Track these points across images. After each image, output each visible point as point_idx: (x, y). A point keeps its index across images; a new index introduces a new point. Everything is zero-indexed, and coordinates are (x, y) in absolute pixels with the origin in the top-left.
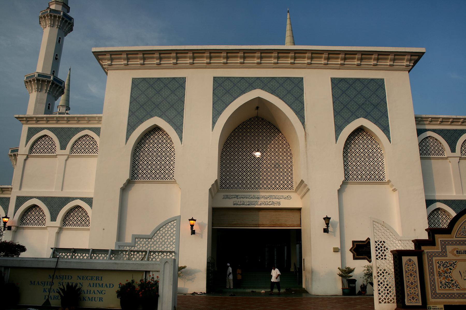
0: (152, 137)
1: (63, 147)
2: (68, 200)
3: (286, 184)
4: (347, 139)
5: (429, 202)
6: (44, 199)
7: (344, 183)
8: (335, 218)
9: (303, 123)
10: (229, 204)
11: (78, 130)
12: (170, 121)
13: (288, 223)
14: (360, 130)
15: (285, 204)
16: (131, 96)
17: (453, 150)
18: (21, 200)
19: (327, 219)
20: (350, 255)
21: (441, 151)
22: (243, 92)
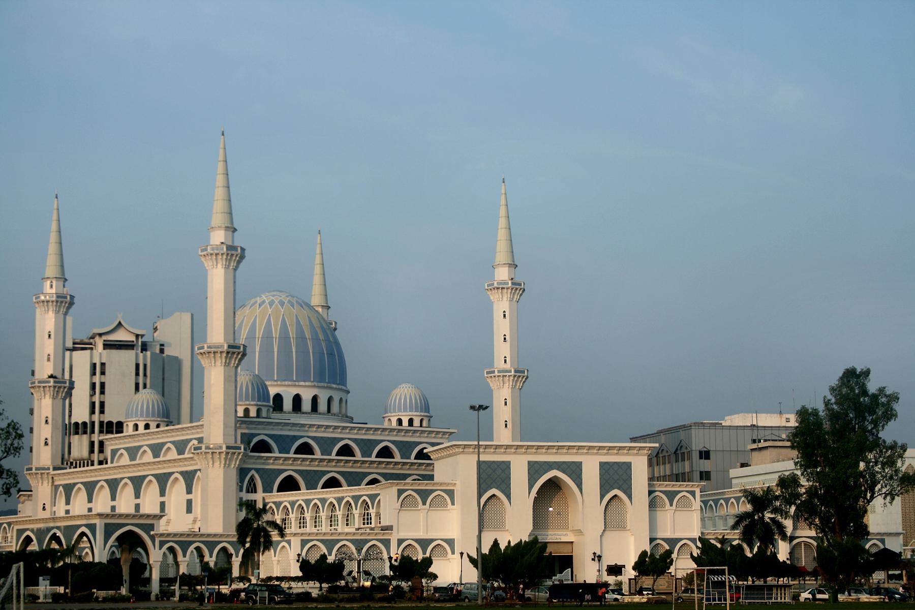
1: (424, 504)
2: (432, 540)
3: (566, 527)
5: (652, 540)
11: (433, 491)
13: (564, 551)
15: (564, 539)
17: (671, 505)
18: (400, 541)
19: (594, 553)
21: (663, 506)
22: (546, 472)
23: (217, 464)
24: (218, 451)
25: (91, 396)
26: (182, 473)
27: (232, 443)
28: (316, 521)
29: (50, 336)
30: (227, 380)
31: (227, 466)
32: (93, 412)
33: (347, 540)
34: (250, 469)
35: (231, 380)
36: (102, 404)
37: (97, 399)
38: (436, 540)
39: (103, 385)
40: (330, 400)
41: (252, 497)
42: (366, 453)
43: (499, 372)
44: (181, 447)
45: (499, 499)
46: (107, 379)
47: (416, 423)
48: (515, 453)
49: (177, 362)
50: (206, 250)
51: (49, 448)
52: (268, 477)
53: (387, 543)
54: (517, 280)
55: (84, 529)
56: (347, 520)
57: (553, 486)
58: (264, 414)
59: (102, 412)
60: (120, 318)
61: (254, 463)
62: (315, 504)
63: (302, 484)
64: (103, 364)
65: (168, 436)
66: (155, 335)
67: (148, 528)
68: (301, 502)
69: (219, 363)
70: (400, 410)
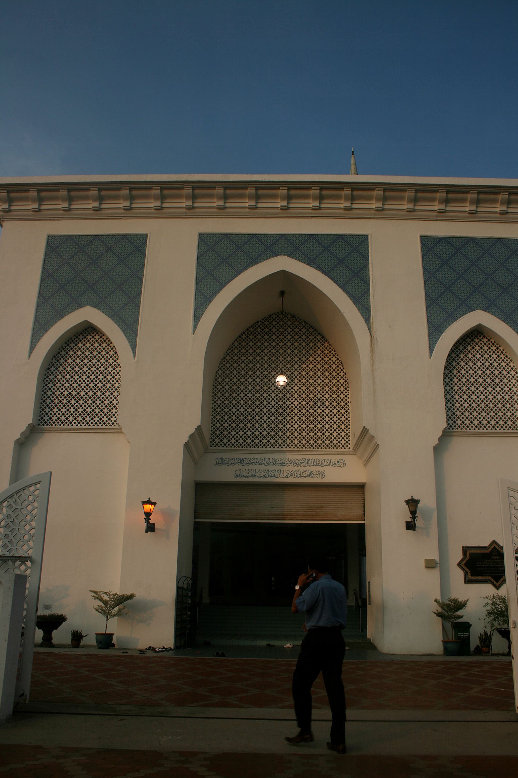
0: (80, 345)
4: (452, 351)
7: (447, 434)
8: (428, 502)
9: (367, 319)
10: (227, 474)
12: (115, 315)
13: (337, 512)
14: (476, 334)
15: (334, 475)
16: (43, 268)
20: (458, 575)
22: (254, 261)
48: (159, 213)
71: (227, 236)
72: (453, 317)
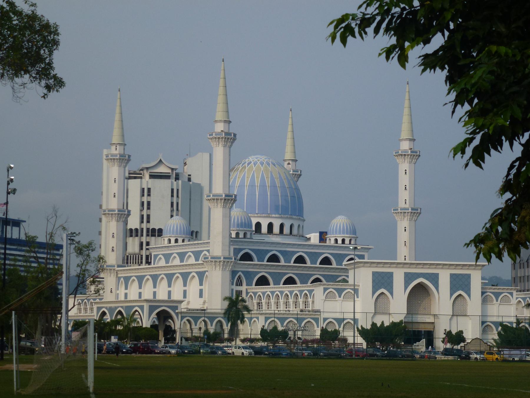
1: (340, 297)
6: (335, 319)
11: (345, 289)
13: (429, 328)
15: (428, 320)
17: (497, 301)
18: (325, 319)
21: (492, 301)
22: (416, 279)
23: (218, 268)
24: (218, 260)
25: (141, 210)
26: (197, 273)
27: (227, 255)
28: (277, 304)
29: (115, 181)
30: (224, 216)
31: (223, 270)
32: (142, 222)
33: (293, 318)
34: (238, 272)
35: (228, 217)
36: (148, 216)
37: (145, 213)
38: (347, 319)
39: (149, 203)
40: (291, 227)
41: (239, 288)
42: (313, 262)
43: (401, 209)
44: (197, 255)
45: (386, 295)
46: (152, 199)
47: (347, 241)
49: (199, 187)
50: (212, 135)
51: (114, 253)
52: (249, 275)
53: (317, 320)
54: (416, 149)
55: (137, 308)
56: (296, 305)
57: (421, 287)
58: (248, 236)
59: (148, 222)
60: (161, 157)
61: (241, 268)
62: (277, 294)
63: (271, 281)
64: (149, 190)
65: (190, 248)
66: (185, 167)
67: (175, 308)
68: (269, 293)
69: (219, 205)
70: (336, 234)
71: (410, 273)
72: (455, 292)
